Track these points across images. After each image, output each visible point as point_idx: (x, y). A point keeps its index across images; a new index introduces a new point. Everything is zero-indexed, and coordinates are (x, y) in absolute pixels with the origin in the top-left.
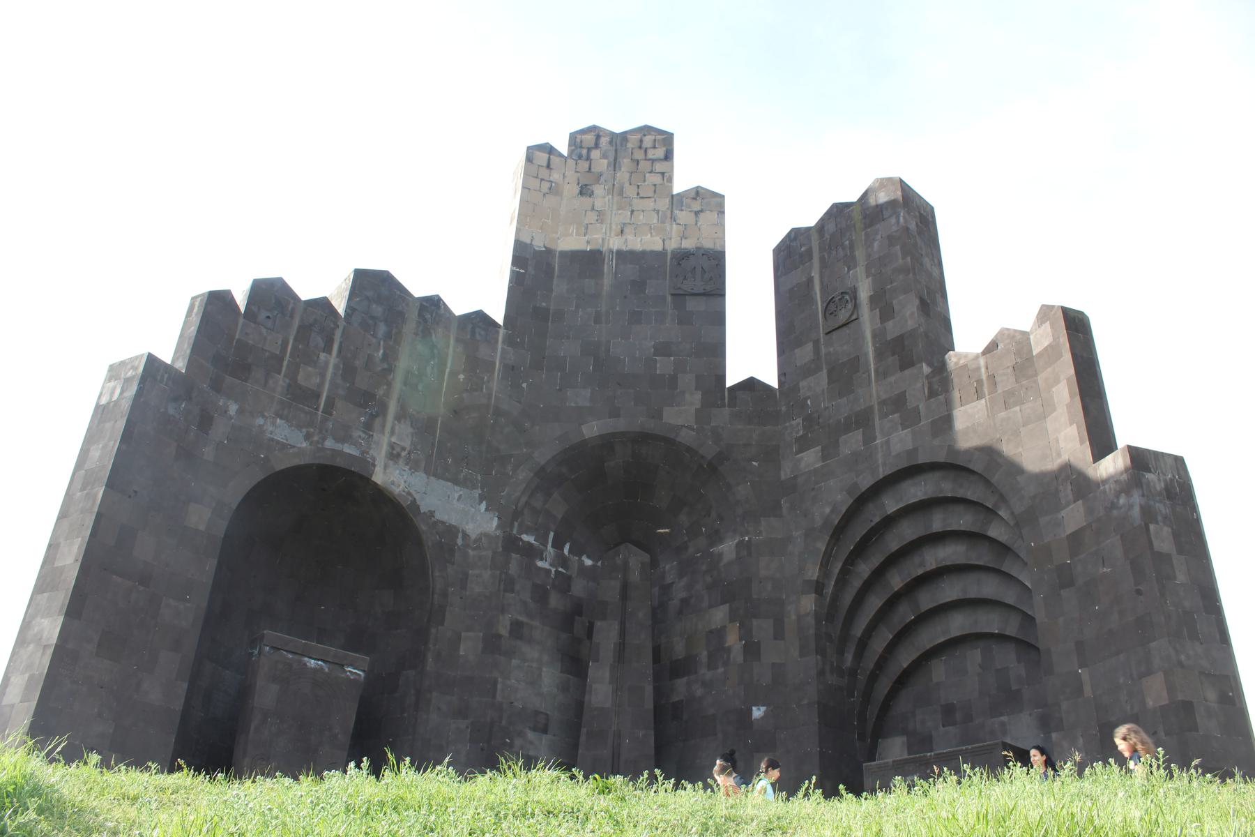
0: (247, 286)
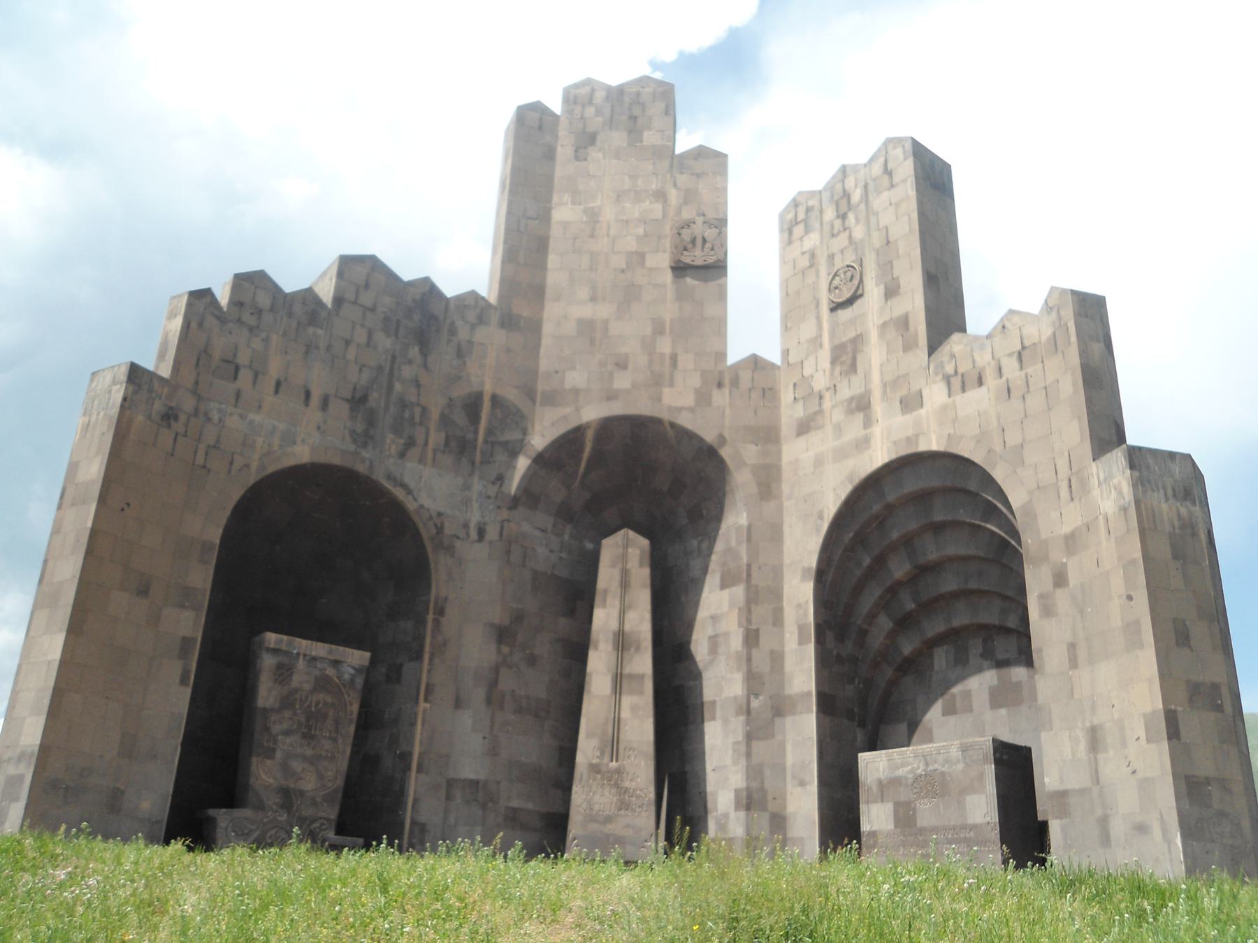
0: (229, 278)
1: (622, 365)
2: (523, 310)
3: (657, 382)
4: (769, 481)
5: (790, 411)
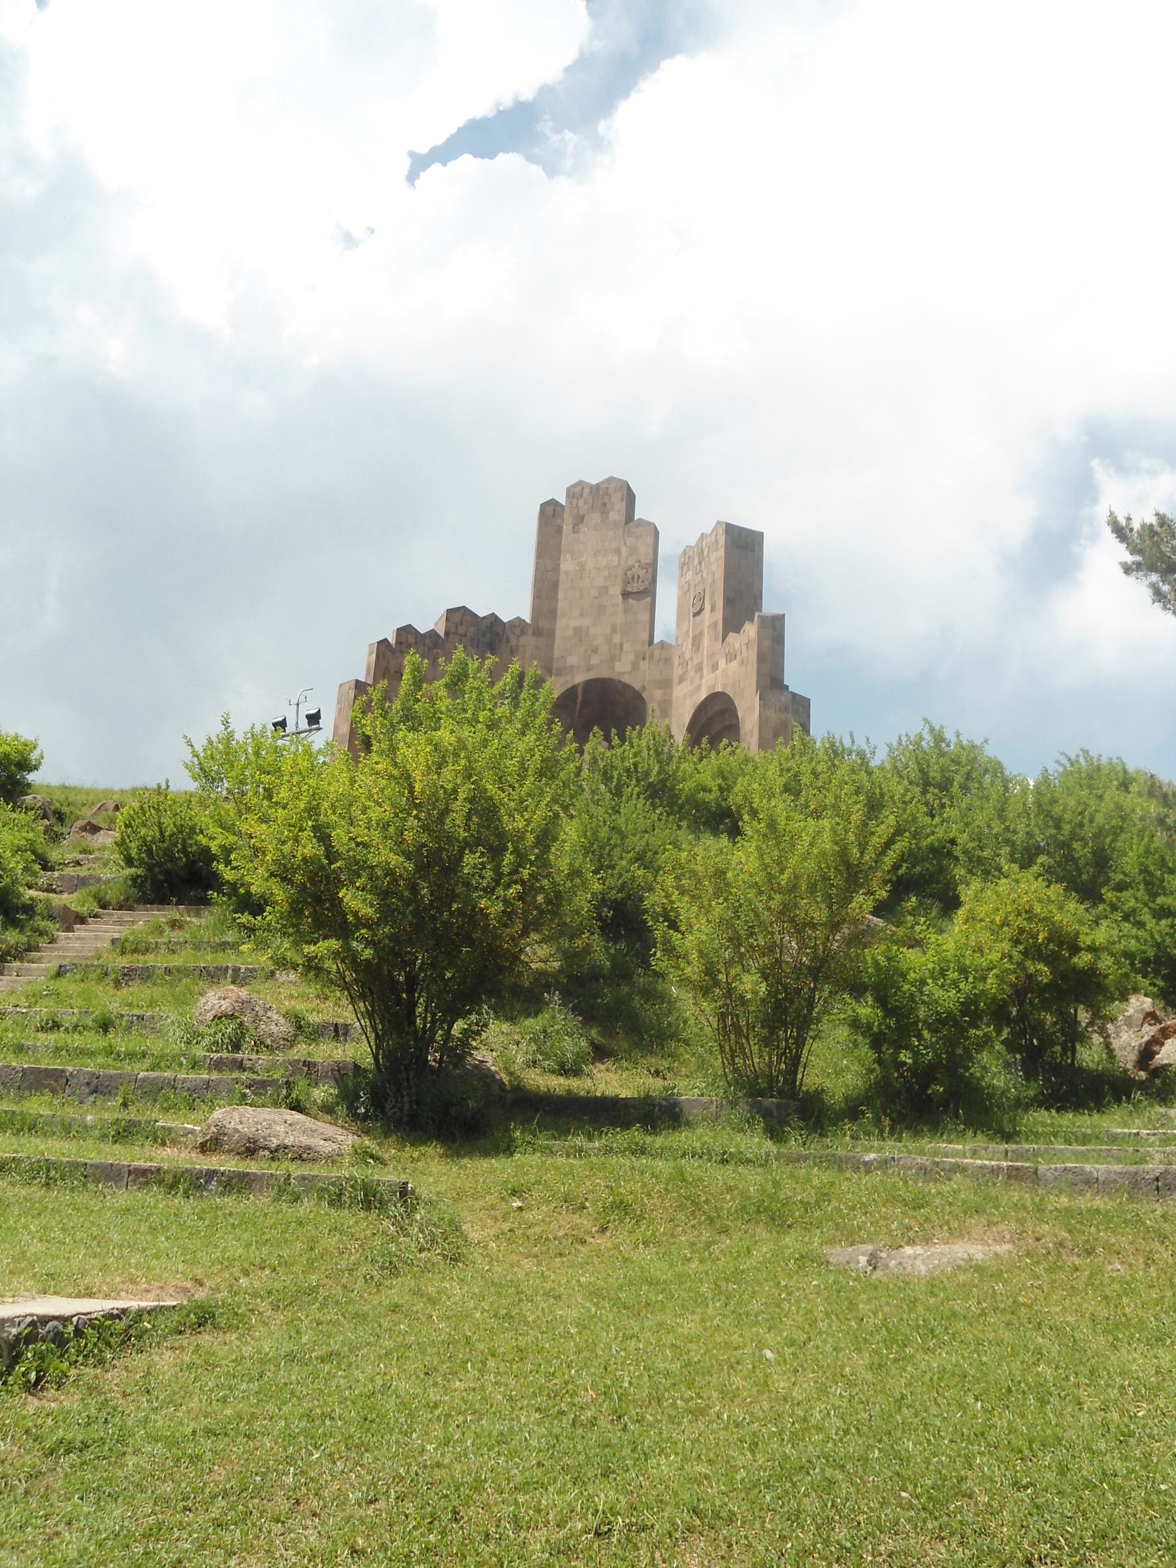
1: (595, 651)
2: (544, 624)
3: (613, 659)
4: (666, 707)
5: (677, 671)
